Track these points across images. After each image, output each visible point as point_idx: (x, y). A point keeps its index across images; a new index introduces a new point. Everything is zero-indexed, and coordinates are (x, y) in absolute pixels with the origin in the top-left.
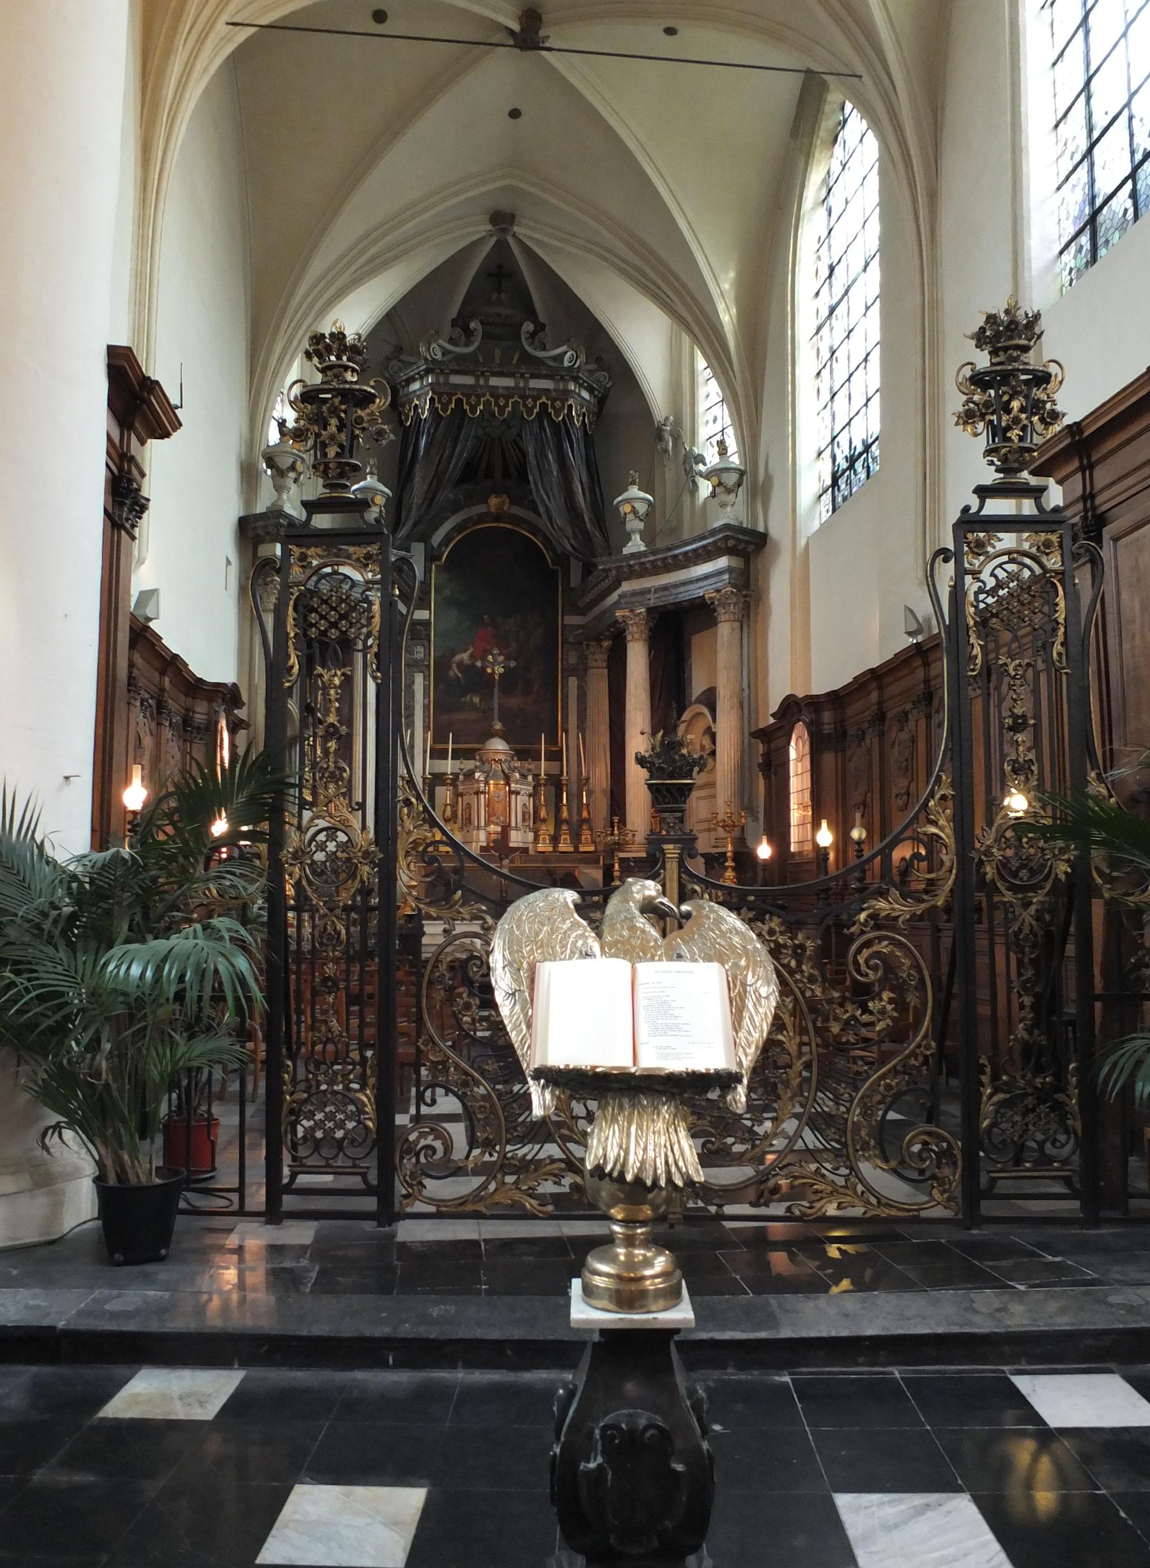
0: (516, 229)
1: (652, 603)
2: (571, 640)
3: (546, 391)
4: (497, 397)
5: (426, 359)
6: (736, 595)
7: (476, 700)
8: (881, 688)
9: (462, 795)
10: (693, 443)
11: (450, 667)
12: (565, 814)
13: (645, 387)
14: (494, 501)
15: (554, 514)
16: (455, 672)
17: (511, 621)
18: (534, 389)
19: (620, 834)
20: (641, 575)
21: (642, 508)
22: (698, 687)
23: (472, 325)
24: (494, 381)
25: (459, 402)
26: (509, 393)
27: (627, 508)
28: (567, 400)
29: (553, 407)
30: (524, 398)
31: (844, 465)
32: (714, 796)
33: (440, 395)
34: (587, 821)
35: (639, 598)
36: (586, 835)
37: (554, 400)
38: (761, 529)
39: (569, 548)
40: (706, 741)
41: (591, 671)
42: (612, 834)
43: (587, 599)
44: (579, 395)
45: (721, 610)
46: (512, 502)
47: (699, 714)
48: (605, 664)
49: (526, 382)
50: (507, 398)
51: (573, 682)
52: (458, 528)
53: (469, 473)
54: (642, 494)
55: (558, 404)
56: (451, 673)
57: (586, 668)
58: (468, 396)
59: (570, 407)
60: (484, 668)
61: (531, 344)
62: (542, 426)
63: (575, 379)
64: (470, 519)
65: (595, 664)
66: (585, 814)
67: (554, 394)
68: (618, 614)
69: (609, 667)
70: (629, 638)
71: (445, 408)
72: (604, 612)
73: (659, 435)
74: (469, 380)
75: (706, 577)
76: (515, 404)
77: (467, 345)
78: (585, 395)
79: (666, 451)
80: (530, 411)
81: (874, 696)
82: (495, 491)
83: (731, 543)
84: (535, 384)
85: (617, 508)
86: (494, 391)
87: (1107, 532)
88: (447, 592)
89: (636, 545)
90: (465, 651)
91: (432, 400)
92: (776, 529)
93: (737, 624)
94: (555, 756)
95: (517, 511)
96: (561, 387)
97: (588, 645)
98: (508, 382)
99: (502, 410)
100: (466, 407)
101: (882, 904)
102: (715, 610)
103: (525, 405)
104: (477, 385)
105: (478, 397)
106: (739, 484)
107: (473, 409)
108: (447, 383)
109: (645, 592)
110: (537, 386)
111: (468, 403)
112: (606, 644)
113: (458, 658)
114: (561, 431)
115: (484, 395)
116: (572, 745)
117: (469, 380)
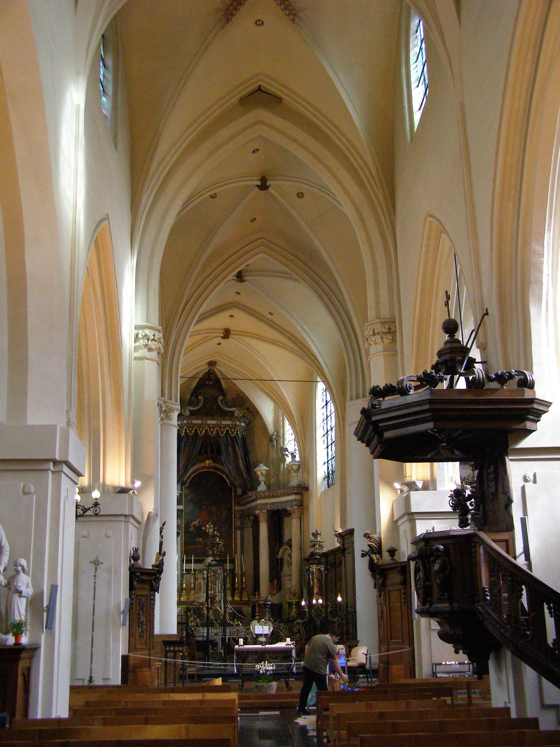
0: (217, 367)
1: (269, 509)
2: (238, 516)
3: (228, 425)
4: (210, 428)
5: (184, 416)
6: (298, 509)
7: (201, 540)
8: (335, 555)
9: (197, 579)
10: (284, 444)
11: (190, 527)
12: (237, 586)
13: (265, 419)
14: (207, 462)
15: (232, 471)
16: (192, 529)
17: (214, 508)
18: (223, 425)
19: (258, 598)
20: (264, 498)
21: (264, 472)
22: (286, 538)
23: (200, 397)
24: (209, 422)
25: (196, 430)
26: (214, 426)
27: (259, 473)
28: (236, 428)
29: (231, 431)
30: (220, 428)
31: (331, 472)
32: (291, 580)
33: (189, 428)
34: (245, 588)
35: (264, 507)
36: (245, 594)
37: (231, 429)
38: (307, 486)
39: (237, 484)
40: (289, 559)
41: (246, 529)
42: (256, 598)
43: (244, 502)
44: (241, 425)
45: (293, 514)
46: (214, 462)
47: (286, 549)
48: (251, 526)
49: (221, 422)
50: (214, 428)
51: (239, 533)
52: (193, 472)
53: (199, 454)
54: (265, 468)
55: (233, 430)
56: (191, 529)
57: (244, 528)
58: (199, 428)
59: (237, 431)
60: (205, 530)
61: (222, 404)
62: (227, 438)
63: (239, 421)
64: (198, 469)
65: (247, 526)
66: (244, 586)
67: (231, 426)
68: (256, 512)
69: (252, 527)
70: (260, 521)
71: (191, 432)
72: (250, 508)
73: (271, 440)
74: (200, 422)
75: (287, 501)
76: (217, 430)
77: (198, 406)
78: (243, 424)
79: (273, 446)
80: (222, 433)
81: (333, 557)
82: (209, 459)
83: (296, 491)
84: (224, 422)
85: (255, 472)
86: (209, 425)
87: (346, 552)
88: (189, 497)
89: (262, 487)
90: (196, 520)
91: (186, 430)
92: (310, 487)
93: (299, 520)
94: (232, 561)
95: (215, 465)
96: (234, 423)
97: (244, 519)
98: (214, 422)
99: (212, 433)
100: (198, 432)
101: (298, 621)
102: (291, 514)
103: (221, 431)
104: (203, 424)
105: (203, 428)
106: (298, 469)
107: (201, 433)
108: (191, 423)
109: (266, 504)
110: (224, 423)
111: (199, 430)
112: (252, 518)
113: (193, 523)
114: (234, 440)
115: (205, 427)
116: (239, 558)
117: (200, 422)
